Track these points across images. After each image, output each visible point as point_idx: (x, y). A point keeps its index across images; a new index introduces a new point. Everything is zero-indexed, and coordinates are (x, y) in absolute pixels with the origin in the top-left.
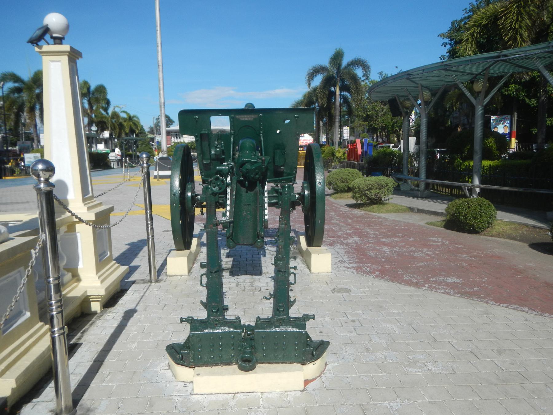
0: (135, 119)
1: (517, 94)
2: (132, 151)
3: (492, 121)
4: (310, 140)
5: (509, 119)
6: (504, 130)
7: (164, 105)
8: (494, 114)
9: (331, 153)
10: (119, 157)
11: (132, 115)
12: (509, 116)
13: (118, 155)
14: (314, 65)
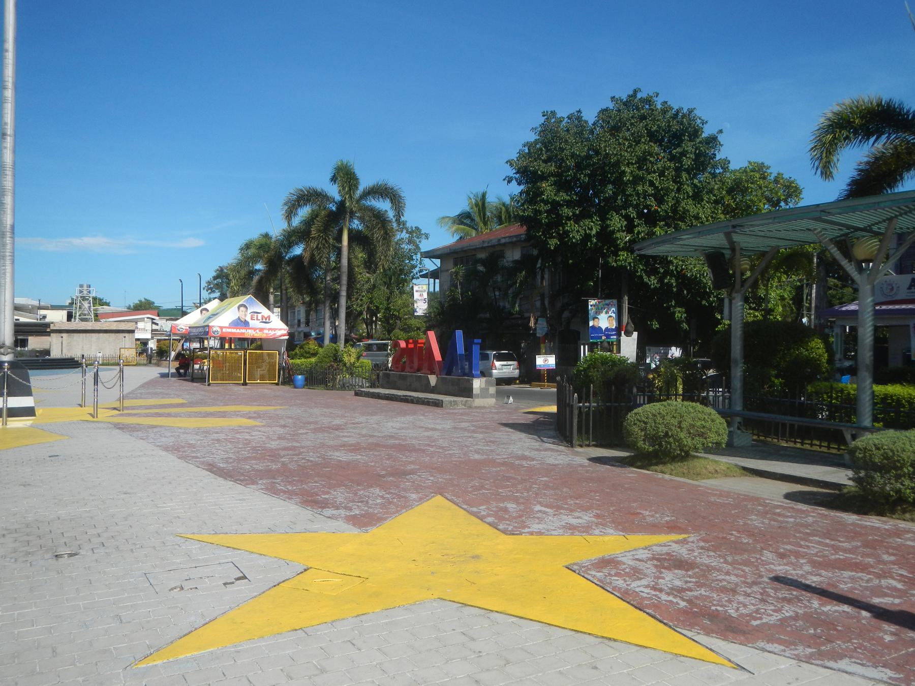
1: (634, 267)
3: (590, 307)
4: (280, 329)
5: (615, 305)
6: (609, 323)
7: (13, 232)
8: (594, 296)
9: (332, 355)
12: (615, 301)
14: (300, 187)
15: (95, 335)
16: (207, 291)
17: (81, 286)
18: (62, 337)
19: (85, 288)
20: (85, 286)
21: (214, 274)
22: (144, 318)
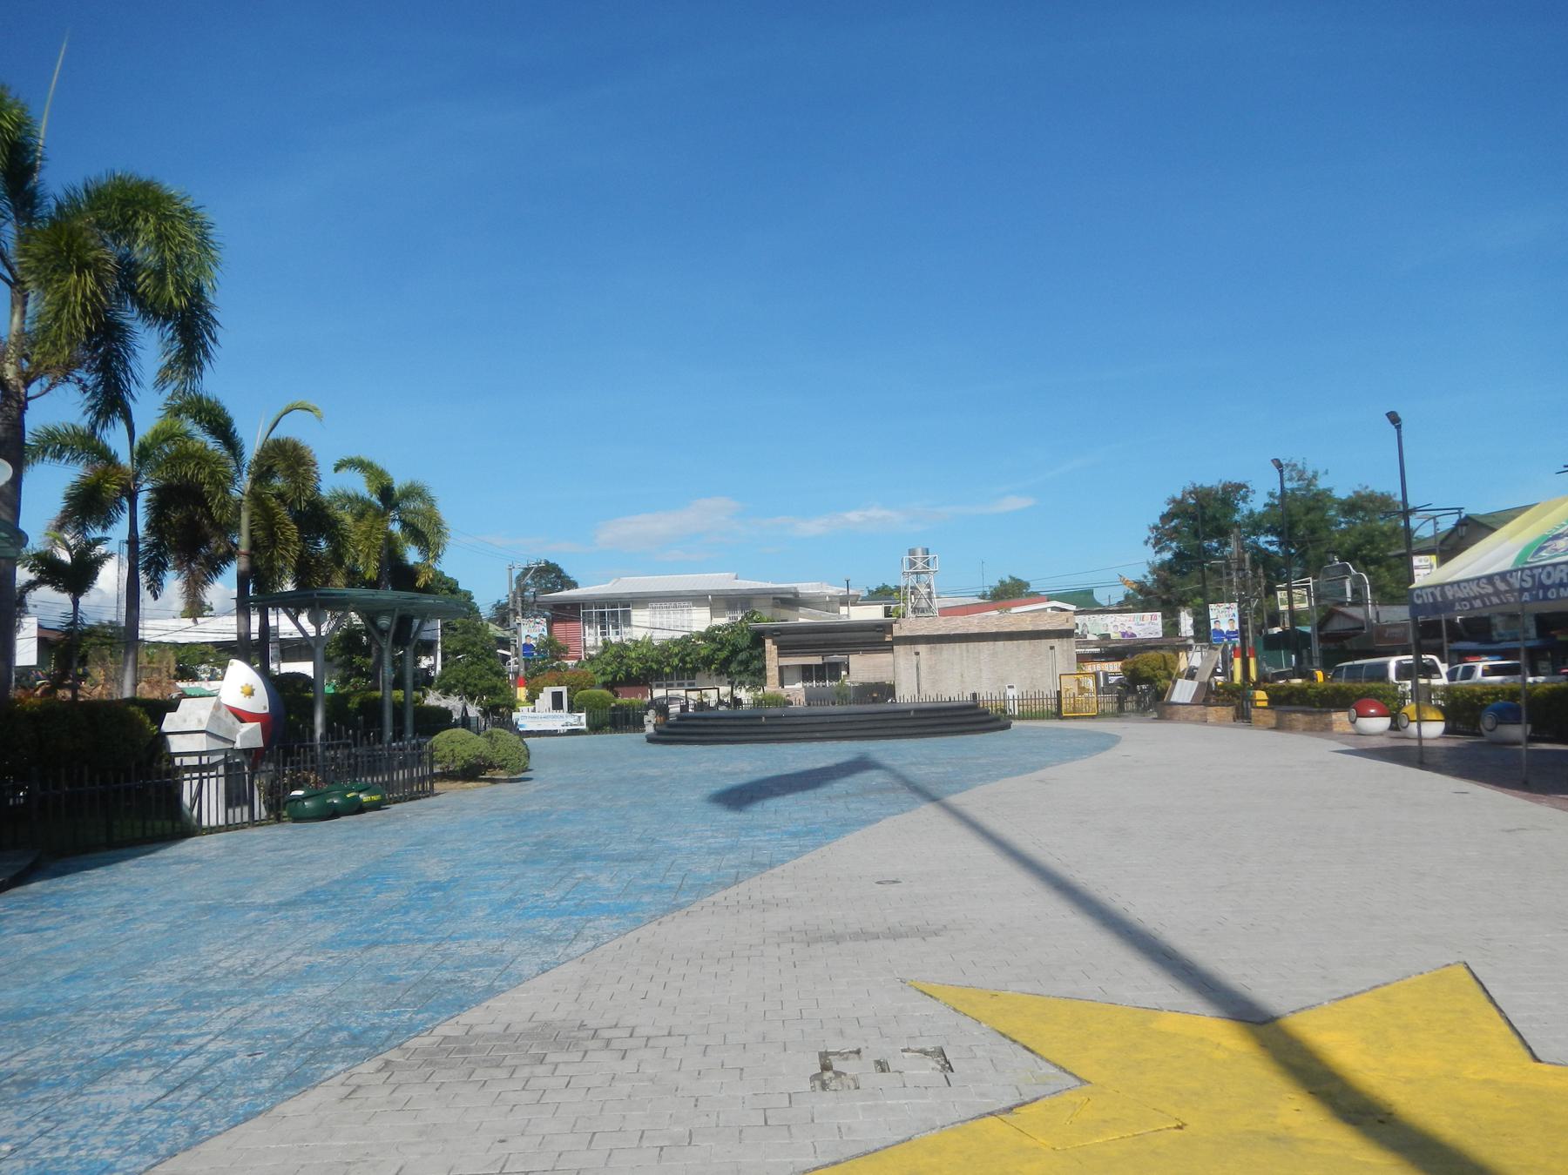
10: (248, 735)
11: (399, 483)
13: (242, 716)
15: (986, 647)
16: (1154, 547)
17: (912, 552)
18: (917, 654)
19: (920, 555)
20: (919, 551)
21: (1166, 509)
22: (1045, 610)
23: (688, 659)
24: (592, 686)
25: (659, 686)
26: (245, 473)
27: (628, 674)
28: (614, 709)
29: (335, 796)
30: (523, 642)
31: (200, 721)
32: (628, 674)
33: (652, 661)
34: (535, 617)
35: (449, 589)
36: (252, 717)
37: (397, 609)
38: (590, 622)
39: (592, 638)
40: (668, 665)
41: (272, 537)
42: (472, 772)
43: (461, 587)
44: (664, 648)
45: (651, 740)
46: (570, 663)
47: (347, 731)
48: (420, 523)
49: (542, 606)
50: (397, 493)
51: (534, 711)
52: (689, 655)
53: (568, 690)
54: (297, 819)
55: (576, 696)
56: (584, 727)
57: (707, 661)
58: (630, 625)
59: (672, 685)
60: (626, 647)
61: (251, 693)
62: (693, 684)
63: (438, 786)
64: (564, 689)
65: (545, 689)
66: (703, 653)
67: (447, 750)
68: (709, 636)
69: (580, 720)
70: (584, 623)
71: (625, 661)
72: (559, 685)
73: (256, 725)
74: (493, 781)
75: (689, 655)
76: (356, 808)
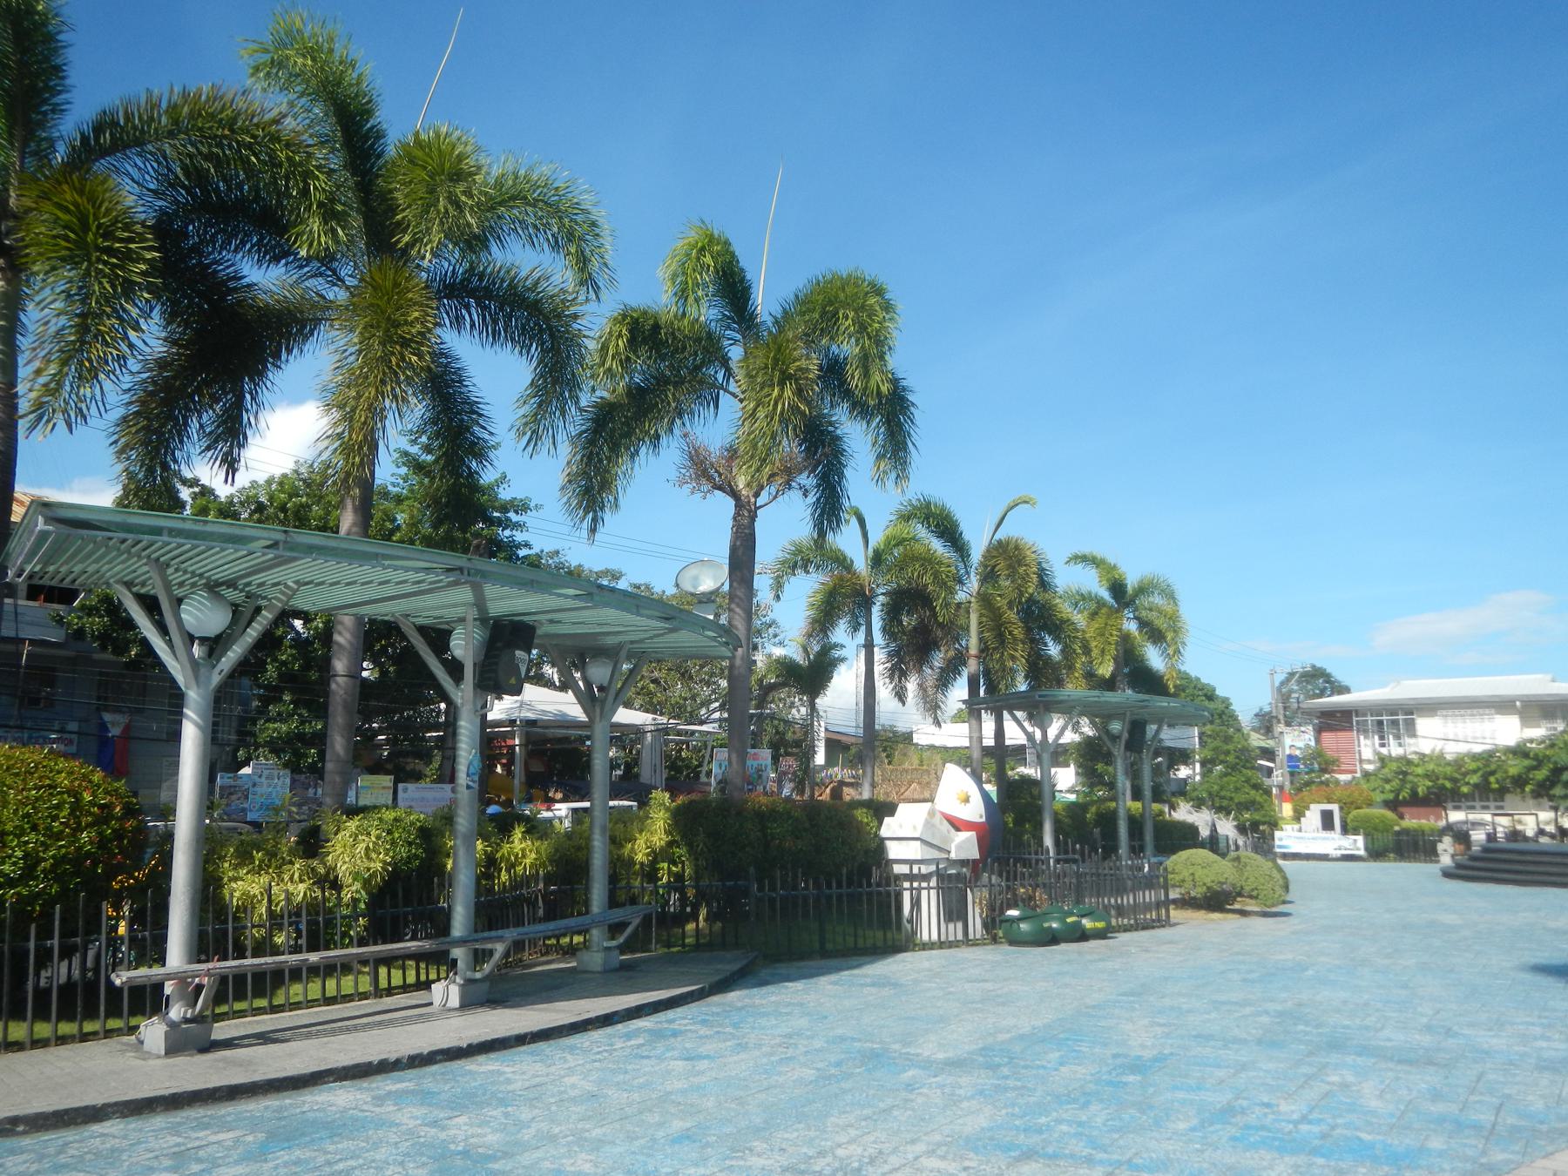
0: (1157, 600)
2: (1137, 795)
13: (957, 824)
23: (1492, 779)
24: (1370, 804)
25: (1457, 808)
26: (972, 574)
27: (1414, 793)
28: (1398, 833)
29: (1053, 919)
30: (1288, 752)
31: (915, 827)
32: (1414, 793)
33: (1446, 779)
34: (1300, 725)
35: (1205, 695)
36: (969, 826)
37: (1128, 714)
38: (1365, 732)
39: (1368, 748)
40: (1468, 783)
41: (1000, 637)
42: (1216, 901)
43: (1220, 692)
44: (1458, 762)
45: (1447, 874)
46: (1343, 777)
47: (1074, 846)
48: (1161, 623)
49: (1308, 714)
50: (1130, 589)
51: (1300, 830)
52: (1493, 773)
53: (1341, 809)
54: (1012, 943)
55: (1351, 816)
56: (1362, 852)
57: (1519, 782)
58: (1413, 734)
59: (1473, 808)
60: (1409, 762)
61: (967, 800)
62: (1501, 808)
63: (1175, 914)
64: (1335, 808)
65: (1312, 806)
66: (1513, 771)
67: (1186, 874)
68: (1520, 751)
69: (1357, 844)
70: (1358, 731)
71: (1410, 778)
72: (1329, 802)
73: (970, 835)
74: (1243, 913)
75: (1493, 773)
76: (1078, 935)
